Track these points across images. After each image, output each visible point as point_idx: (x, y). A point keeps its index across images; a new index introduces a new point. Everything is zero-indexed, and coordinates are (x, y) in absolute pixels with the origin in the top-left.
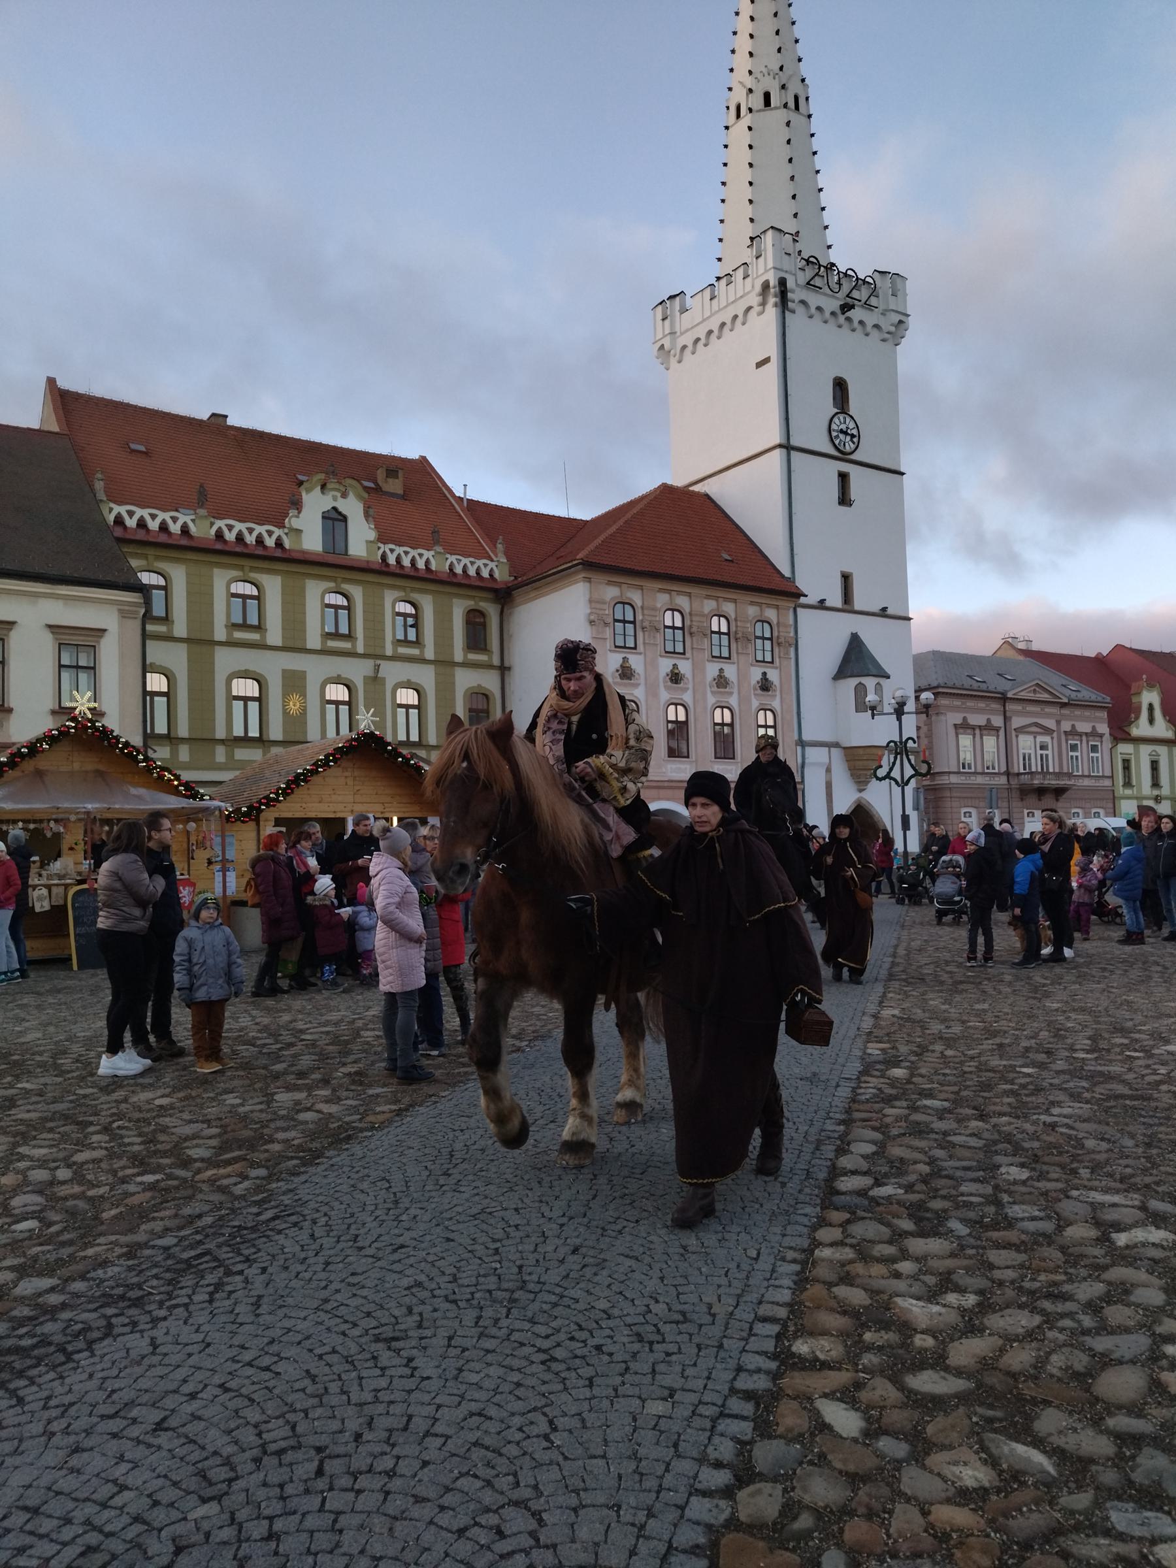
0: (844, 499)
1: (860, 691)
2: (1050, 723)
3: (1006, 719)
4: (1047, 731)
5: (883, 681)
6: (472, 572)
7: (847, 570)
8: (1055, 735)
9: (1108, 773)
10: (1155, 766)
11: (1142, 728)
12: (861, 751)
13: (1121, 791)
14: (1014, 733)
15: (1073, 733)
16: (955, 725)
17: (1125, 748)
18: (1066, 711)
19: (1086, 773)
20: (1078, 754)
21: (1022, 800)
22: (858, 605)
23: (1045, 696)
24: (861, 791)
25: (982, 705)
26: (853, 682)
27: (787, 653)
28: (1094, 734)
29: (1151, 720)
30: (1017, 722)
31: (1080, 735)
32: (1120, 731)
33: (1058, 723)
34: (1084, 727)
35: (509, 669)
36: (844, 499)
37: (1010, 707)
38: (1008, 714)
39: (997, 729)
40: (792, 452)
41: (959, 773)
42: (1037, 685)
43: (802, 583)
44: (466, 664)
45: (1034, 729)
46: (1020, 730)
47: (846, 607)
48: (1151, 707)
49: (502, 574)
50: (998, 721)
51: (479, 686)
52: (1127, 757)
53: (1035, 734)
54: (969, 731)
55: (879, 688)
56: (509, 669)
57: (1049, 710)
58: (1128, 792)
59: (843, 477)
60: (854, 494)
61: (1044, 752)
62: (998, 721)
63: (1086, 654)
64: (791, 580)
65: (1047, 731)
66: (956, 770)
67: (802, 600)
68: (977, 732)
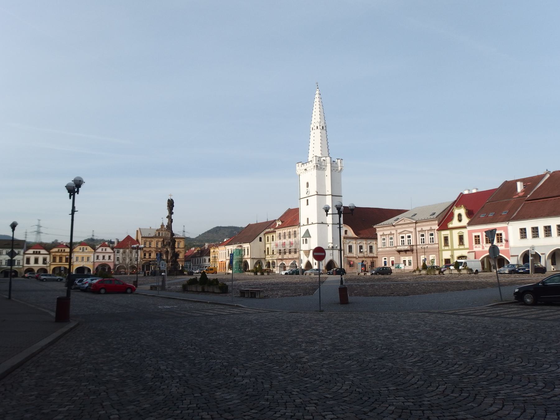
3: (396, 231)
4: (411, 232)
8: (413, 233)
10: (461, 238)
11: (455, 223)
14: (398, 234)
15: (422, 231)
17: (445, 233)
25: (389, 228)
29: (460, 220)
30: (399, 231)
48: (460, 215)
58: (447, 248)
59: (308, 200)
62: (393, 232)
66: (381, 247)
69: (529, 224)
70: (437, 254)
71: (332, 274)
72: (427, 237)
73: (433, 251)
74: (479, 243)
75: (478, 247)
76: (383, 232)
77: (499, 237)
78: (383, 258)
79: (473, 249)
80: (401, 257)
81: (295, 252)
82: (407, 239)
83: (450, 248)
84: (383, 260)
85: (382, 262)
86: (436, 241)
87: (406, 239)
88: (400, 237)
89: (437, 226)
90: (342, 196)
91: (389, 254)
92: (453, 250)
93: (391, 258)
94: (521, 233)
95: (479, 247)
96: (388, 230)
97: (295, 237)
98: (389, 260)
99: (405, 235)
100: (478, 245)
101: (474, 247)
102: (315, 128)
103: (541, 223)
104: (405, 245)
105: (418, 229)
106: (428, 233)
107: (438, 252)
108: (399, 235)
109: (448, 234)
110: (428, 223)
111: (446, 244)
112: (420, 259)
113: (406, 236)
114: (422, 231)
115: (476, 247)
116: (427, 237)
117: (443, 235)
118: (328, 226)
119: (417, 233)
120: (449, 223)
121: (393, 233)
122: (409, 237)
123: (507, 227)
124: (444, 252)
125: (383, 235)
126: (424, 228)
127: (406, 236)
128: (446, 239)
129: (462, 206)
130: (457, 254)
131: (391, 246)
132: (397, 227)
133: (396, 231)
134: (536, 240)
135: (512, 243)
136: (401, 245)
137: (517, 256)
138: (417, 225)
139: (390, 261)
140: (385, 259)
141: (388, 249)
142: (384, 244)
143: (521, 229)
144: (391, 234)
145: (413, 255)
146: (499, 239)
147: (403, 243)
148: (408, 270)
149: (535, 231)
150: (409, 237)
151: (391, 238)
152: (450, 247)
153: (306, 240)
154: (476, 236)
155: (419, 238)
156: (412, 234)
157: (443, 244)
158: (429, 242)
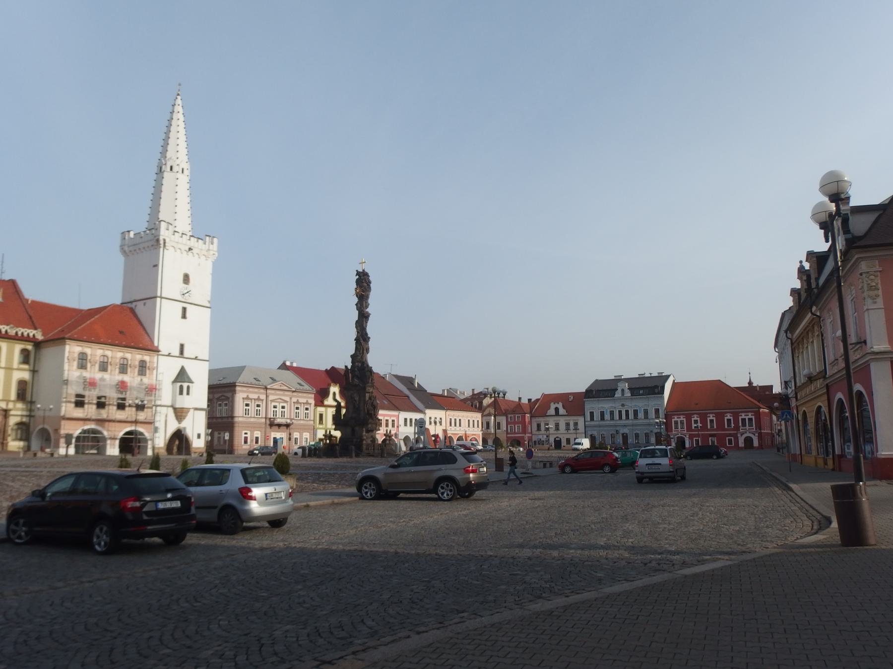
0: (184, 316)
1: (181, 388)
2: (287, 399)
4: (286, 402)
5: (190, 384)
6: (25, 334)
7: (182, 343)
8: (289, 403)
9: (312, 419)
12: (179, 409)
13: (318, 426)
14: (270, 402)
15: (298, 402)
16: (243, 398)
17: (320, 409)
18: (295, 394)
19: (302, 419)
21: (271, 428)
22: (186, 354)
23: (285, 388)
24: (180, 423)
25: (256, 390)
26: (179, 384)
27: (153, 372)
28: (307, 403)
31: (301, 403)
32: (320, 402)
33: (291, 398)
34: (302, 400)
35: (37, 371)
36: (184, 316)
37: (269, 391)
38: (268, 395)
39: (262, 400)
40: (163, 299)
41: (243, 417)
42: (282, 384)
43: (160, 348)
44: (18, 369)
45: (280, 401)
46: (272, 401)
47: (181, 356)
48: (334, 394)
49: (39, 336)
50: (263, 397)
51: (23, 378)
52: (321, 413)
53: (279, 402)
54: (250, 400)
55: (188, 387)
56: (37, 371)
57: (287, 393)
58: (321, 426)
59: (184, 309)
60: (188, 314)
61: (283, 410)
63: (320, 369)
64: (158, 347)
65: (286, 402)
67: (160, 353)
72: (302, 411)
73: (302, 429)
76: (247, 394)
81: (140, 407)
82: (281, 410)
84: (244, 436)
85: (241, 437)
88: (272, 407)
91: (253, 427)
93: (255, 432)
96: (256, 393)
108: (271, 403)
112: (271, 436)
116: (302, 411)
127: (279, 406)
128: (321, 416)
129: (338, 385)
131: (257, 415)
136: (280, 416)
140: (246, 434)
141: (252, 420)
142: (247, 412)
151: (307, 409)
153: (181, 388)
155: (294, 411)
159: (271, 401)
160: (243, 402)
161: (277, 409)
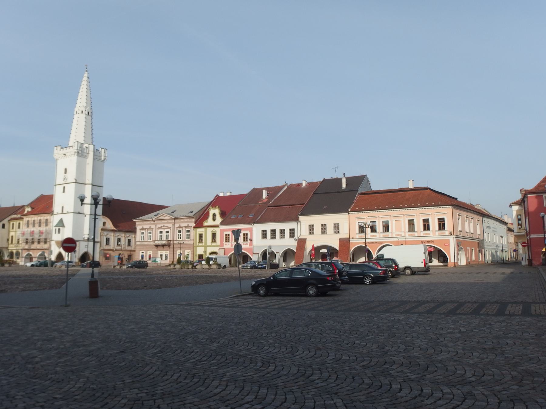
3: (156, 226)
4: (170, 228)
8: (171, 229)
10: (214, 236)
11: (210, 222)
14: (157, 229)
15: (180, 227)
17: (200, 230)
20: (151, 235)
25: (148, 222)
29: (214, 219)
30: (158, 226)
41: (140, 242)
48: (214, 215)
58: (201, 244)
59: (64, 187)
62: (153, 226)
66: (139, 241)
68: (146, 230)
69: (268, 227)
70: (191, 249)
71: (85, 267)
72: (184, 234)
73: (188, 247)
74: (229, 241)
75: (227, 244)
76: (143, 226)
77: (245, 236)
78: (141, 252)
79: (223, 246)
80: (158, 251)
81: (45, 242)
82: (165, 234)
83: (204, 244)
84: (141, 254)
85: (139, 255)
86: (192, 237)
87: (164, 234)
88: (159, 232)
89: (194, 223)
90: (102, 187)
91: (147, 248)
92: (206, 246)
93: (148, 252)
94: (263, 234)
95: (228, 245)
97: (47, 225)
98: (146, 253)
99: (164, 230)
100: (227, 243)
101: (224, 244)
102: (80, 112)
103: (278, 226)
104: (163, 239)
105: (177, 225)
106: (185, 229)
107: (193, 247)
108: (158, 230)
109: (203, 232)
110: (186, 220)
111: (201, 240)
112: (176, 253)
113: (164, 231)
114: (180, 227)
115: (226, 245)
116: (184, 234)
117: (199, 232)
118: (85, 216)
119: (175, 229)
120: (205, 221)
121: (152, 227)
122: (167, 232)
123: (252, 228)
124: (198, 248)
125: (143, 229)
126: (182, 225)
127: (164, 231)
128: (201, 236)
129: (217, 206)
130: (210, 250)
132: (156, 222)
133: (156, 226)
134: (273, 240)
135: (255, 243)
136: (159, 239)
137: (259, 253)
138: (176, 221)
139: (147, 255)
140: (143, 253)
141: (146, 243)
143: (263, 231)
144: (150, 228)
145: (170, 249)
146: (245, 238)
147: (161, 237)
148: (164, 264)
149: (273, 232)
150: (167, 232)
151: (150, 233)
152: (204, 243)
153: (59, 230)
154: (226, 235)
155: (177, 234)
156: (170, 230)
157: (198, 241)
158: (185, 238)
159: (158, 228)
160: (140, 231)
161: (163, 234)
